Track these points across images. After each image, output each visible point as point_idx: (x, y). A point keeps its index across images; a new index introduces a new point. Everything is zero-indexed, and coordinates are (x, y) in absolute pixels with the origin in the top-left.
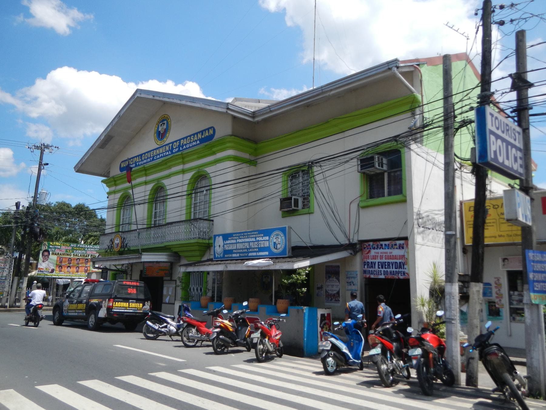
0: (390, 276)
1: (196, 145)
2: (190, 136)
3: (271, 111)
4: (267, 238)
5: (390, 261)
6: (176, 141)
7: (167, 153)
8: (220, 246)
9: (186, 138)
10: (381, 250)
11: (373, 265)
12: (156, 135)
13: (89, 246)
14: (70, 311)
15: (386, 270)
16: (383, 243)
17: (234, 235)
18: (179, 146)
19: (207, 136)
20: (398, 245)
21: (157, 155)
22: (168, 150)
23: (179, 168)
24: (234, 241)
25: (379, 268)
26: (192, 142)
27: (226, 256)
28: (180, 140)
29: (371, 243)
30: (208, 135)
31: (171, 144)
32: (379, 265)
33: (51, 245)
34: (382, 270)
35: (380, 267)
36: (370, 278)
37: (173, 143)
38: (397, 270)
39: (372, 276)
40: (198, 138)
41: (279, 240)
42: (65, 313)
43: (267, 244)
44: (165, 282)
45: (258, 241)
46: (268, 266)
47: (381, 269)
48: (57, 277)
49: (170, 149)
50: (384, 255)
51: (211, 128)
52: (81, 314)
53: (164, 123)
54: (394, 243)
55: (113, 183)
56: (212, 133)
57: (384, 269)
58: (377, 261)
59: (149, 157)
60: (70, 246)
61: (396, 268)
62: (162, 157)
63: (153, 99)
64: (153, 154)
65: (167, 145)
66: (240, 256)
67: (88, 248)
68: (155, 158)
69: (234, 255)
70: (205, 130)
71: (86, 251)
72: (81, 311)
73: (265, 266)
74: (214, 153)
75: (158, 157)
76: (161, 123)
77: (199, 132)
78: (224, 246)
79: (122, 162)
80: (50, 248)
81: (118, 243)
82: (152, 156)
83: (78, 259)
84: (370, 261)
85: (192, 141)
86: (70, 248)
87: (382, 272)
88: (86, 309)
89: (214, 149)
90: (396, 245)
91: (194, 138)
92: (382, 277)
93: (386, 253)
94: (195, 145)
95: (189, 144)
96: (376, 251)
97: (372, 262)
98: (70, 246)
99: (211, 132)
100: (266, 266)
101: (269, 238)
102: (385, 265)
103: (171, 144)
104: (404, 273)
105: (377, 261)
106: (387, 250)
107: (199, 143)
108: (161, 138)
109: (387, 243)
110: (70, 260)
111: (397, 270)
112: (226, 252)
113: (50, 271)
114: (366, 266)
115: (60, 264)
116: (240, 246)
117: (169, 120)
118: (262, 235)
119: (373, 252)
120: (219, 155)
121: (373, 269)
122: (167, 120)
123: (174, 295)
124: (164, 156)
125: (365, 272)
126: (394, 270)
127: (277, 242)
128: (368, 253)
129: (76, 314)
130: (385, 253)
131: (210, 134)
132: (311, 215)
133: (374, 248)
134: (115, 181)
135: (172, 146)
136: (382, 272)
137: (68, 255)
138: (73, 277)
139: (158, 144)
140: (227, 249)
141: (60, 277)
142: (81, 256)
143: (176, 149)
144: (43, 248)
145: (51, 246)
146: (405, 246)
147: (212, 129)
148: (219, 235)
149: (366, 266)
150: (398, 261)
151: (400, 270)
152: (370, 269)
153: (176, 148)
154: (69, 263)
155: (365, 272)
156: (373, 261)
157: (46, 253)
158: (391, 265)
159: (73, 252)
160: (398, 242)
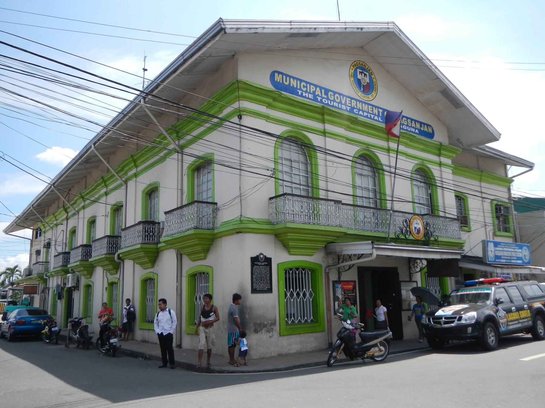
4: (520, 251)
8: (491, 251)
12: (352, 79)
14: (510, 323)
17: (501, 244)
22: (377, 114)
24: (501, 249)
27: (497, 260)
30: (427, 131)
40: (417, 128)
42: (504, 327)
43: (520, 255)
44: (402, 284)
45: (516, 252)
49: (381, 115)
52: (526, 324)
56: (431, 132)
62: (367, 117)
64: (351, 104)
66: (506, 262)
68: (355, 110)
69: (502, 261)
70: (424, 124)
72: (526, 320)
75: (361, 113)
76: (361, 71)
77: (418, 122)
78: (495, 252)
79: (279, 73)
88: (532, 316)
99: (430, 130)
107: (418, 133)
112: (497, 257)
116: (506, 254)
118: (518, 248)
124: (370, 118)
127: (526, 255)
129: (520, 325)
132: (469, 233)
139: (360, 95)
140: (497, 254)
148: (491, 242)
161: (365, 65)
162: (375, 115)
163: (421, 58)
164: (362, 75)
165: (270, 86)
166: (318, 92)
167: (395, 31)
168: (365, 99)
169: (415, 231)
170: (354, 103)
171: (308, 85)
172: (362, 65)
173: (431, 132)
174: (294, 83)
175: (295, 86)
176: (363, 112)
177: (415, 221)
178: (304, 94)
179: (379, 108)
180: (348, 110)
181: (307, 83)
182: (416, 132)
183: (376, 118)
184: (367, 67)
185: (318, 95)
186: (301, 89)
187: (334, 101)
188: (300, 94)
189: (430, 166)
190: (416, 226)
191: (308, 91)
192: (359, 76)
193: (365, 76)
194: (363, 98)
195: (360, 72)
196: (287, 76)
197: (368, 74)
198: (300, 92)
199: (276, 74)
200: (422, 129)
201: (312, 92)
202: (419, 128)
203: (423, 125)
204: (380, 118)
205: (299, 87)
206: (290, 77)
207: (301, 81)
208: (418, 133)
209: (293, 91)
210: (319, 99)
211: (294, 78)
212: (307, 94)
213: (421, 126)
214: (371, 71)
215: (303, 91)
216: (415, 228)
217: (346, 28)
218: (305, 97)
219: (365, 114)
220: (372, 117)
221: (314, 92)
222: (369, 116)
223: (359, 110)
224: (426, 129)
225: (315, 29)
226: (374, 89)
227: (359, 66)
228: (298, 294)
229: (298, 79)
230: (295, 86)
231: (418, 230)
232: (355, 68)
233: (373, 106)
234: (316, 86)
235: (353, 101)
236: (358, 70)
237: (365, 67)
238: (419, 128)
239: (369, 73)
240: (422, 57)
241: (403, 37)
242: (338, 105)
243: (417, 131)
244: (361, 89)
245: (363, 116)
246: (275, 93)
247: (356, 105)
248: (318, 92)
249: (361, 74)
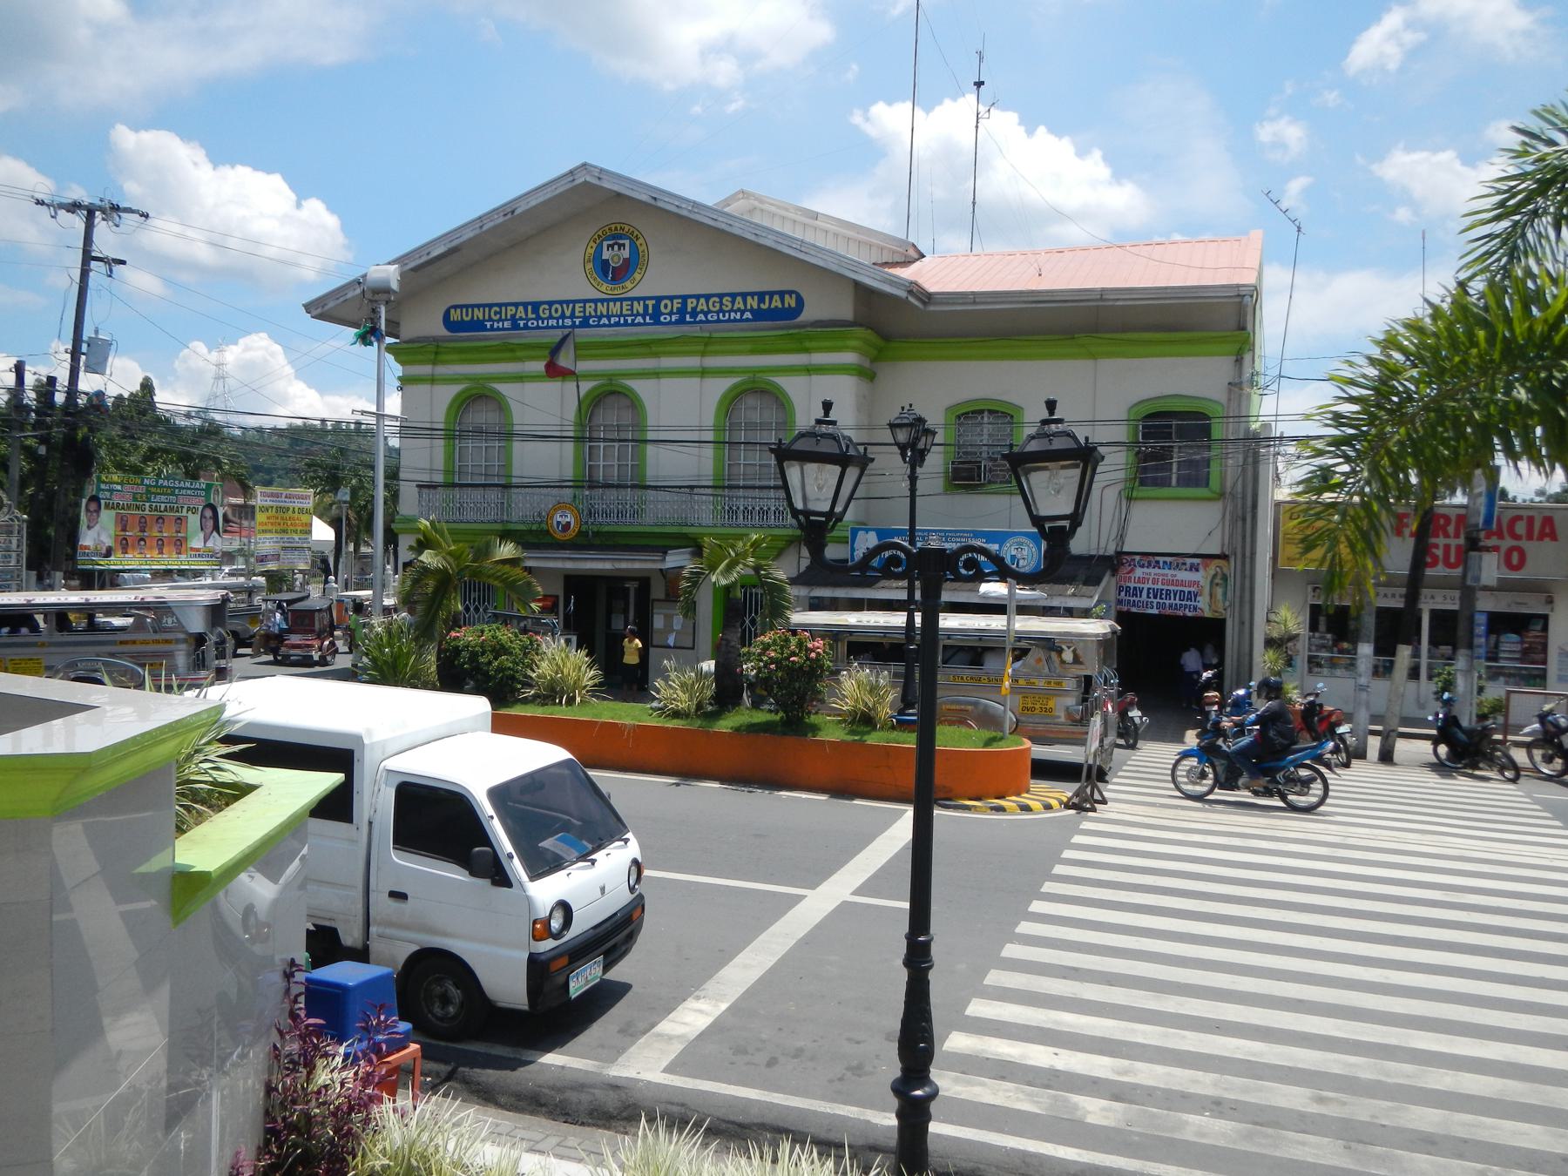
0: (1168, 612)
1: (741, 320)
2: (721, 296)
3: (975, 303)
5: (1171, 588)
6: (671, 298)
7: (639, 319)
9: (708, 297)
10: (1156, 570)
11: (1137, 592)
12: (590, 266)
13: (182, 485)
15: (1161, 601)
16: (1162, 559)
18: (682, 311)
19: (776, 307)
20: (1188, 566)
21: (600, 318)
22: (641, 311)
23: (693, 362)
25: (1148, 597)
26: (729, 312)
28: (685, 298)
29: (1137, 558)
30: (780, 306)
31: (654, 302)
32: (1148, 593)
33: (104, 482)
34: (1155, 601)
35: (1151, 595)
36: (1129, 613)
37: (659, 299)
38: (1183, 603)
39: (1134, 610)
40: (749, 307)
41: (1025, 553)
46: (1035, 600)
47: (1152, 600)
48: (121, 567)
49: (650, 311)
50: (1161, 578)
51: (790, 293)
53: (624, 245)
54: (1181, 560)
55: (432, 357)
56: (793, 304)
57: (1158, 600)
58: (1146, 586)
59: (568, 313)
60: (142, 484)
61: (1180, 600)
62: (617, 324)
63: (651, 205)
64: (584, 312)
65: (638, 299)
67: (180, 488)
68: (591, 322)
70: (772, 294)
71: (176, 495)
73: (1026, 600)
74: (807, 351)
76: (611, 242)
77: (752, 294)
79: (455, 307)
80: (103, 490)
81: (569, 523)
82: (577, 314)
83: (160, 517)
84: (1132, 585)
85: (724, 307)
86: (142, 489)
87: (1155, 605)
89: (807, 344)
90: (1184, 564)
91: (733, 302)
92: (1155, 611)
93: (1167, 575)
94: (735, 320)
95: (718, 313)
96: (1145, 570)
97: (1135, 588)
98: (142, 484)
99: (791, 302)
100: (1030, 600)
101: (1000, 547)
102: (1161, 594)
103: (654, 302)
104: (1195, 608)
105: (1146, 586)
106: (1166, 571)
107: (750, 317)
109: (1168, 559)
110: (143, 520)
111: (1183, 603)
113: (104, 551)
114: (1123, 594)
115: (123, 533)
117: (641, 240)
119: (1139, 572)
120: (819, 358)
121: (1137, 599)
122: (630, 238)
123: (691, 631)
125: (1120, 602)
126: (1178, 601)
128: (1128, 573)
130: (1163, 575)
131: (786, 305)
133: (1143, 566)
134: (436, 353)
135: (656, 307)
136: (1155, 605)
137: (138, 508)
138: (169, 567)
139: (603, 289)
141: (127, 567)
142: (166, 510)
143: (671, 314)
144: (90, 490)
145: (103, 486)
146: (1201, 567)
147: (794, 296)
149: (1123, 594)
150: (1186, 590)
151: (1188, 603)
152: (1132, 599)
153: (671, 314)
154: (141, 531)
155: (1120, 602)
156: (1137, 585)
157: (93, 506)
158: (1172, 595)
159: (149, 500)
160: (1189, 561)
162: (638, 314)
163: (652, 202)
164: (613, 249)
165: (443, 332)
166: (521, 312)
167: (589, 179)
170: (590, 308)
171: (503, 309)
173: (793, 304)
174: (478, 314)
175: (481, 318)
176: (609, 317)
178: (496, 325)
179: (644, 299)
180: (577, 323)
181: (500, 305)
182: (744, 317)
183: (639, 319)
184: (627, 228)
185: (521, 319)
186: (490, 319)
187: (551, 317)
188: (488, 327)
189: (776, 380)
190: (559, 519)
191: (503, 317)
192: (606, 255)
193: (619, 249)
195: (609, 246)
196: (467, 306)
197: (627, 242)
198: (488, 324)
199: (452, 311)
200: (764, 306)
201: (509, 317)
202: (755, 306)
203: (767, 298)
204: (648, 318)
205: (487, 317)
206: (473, 306)
207: (490, 306)
208: (750, 317)
209: (478, 325)
210: (522, 323)
211: (478, 306)
212: (501, 325)
213: (761, 300)
214: (636, 233)
215: (493, 321)
217: (481, 227)
218: (498, 329)
219: (613, 320)
220: (630, 321)
221: (513, 316)
222: (622, 322)
223: (602, 316)
224: (776, 303)
225: (428, 254)
228: (477, 609)
229: (484, 306)
230: (481, 318)
232: (598, 241)
233: (632, 299)
234: (516, 305)
235: (588, 305)
238: (755, 306)
239: (630, 238)
240: (655, 199)
242: (558, 323)
243: (748, 315)
244: (607, 277)
245: (610, 325)
247: (596, 310)
248: (521, 312)
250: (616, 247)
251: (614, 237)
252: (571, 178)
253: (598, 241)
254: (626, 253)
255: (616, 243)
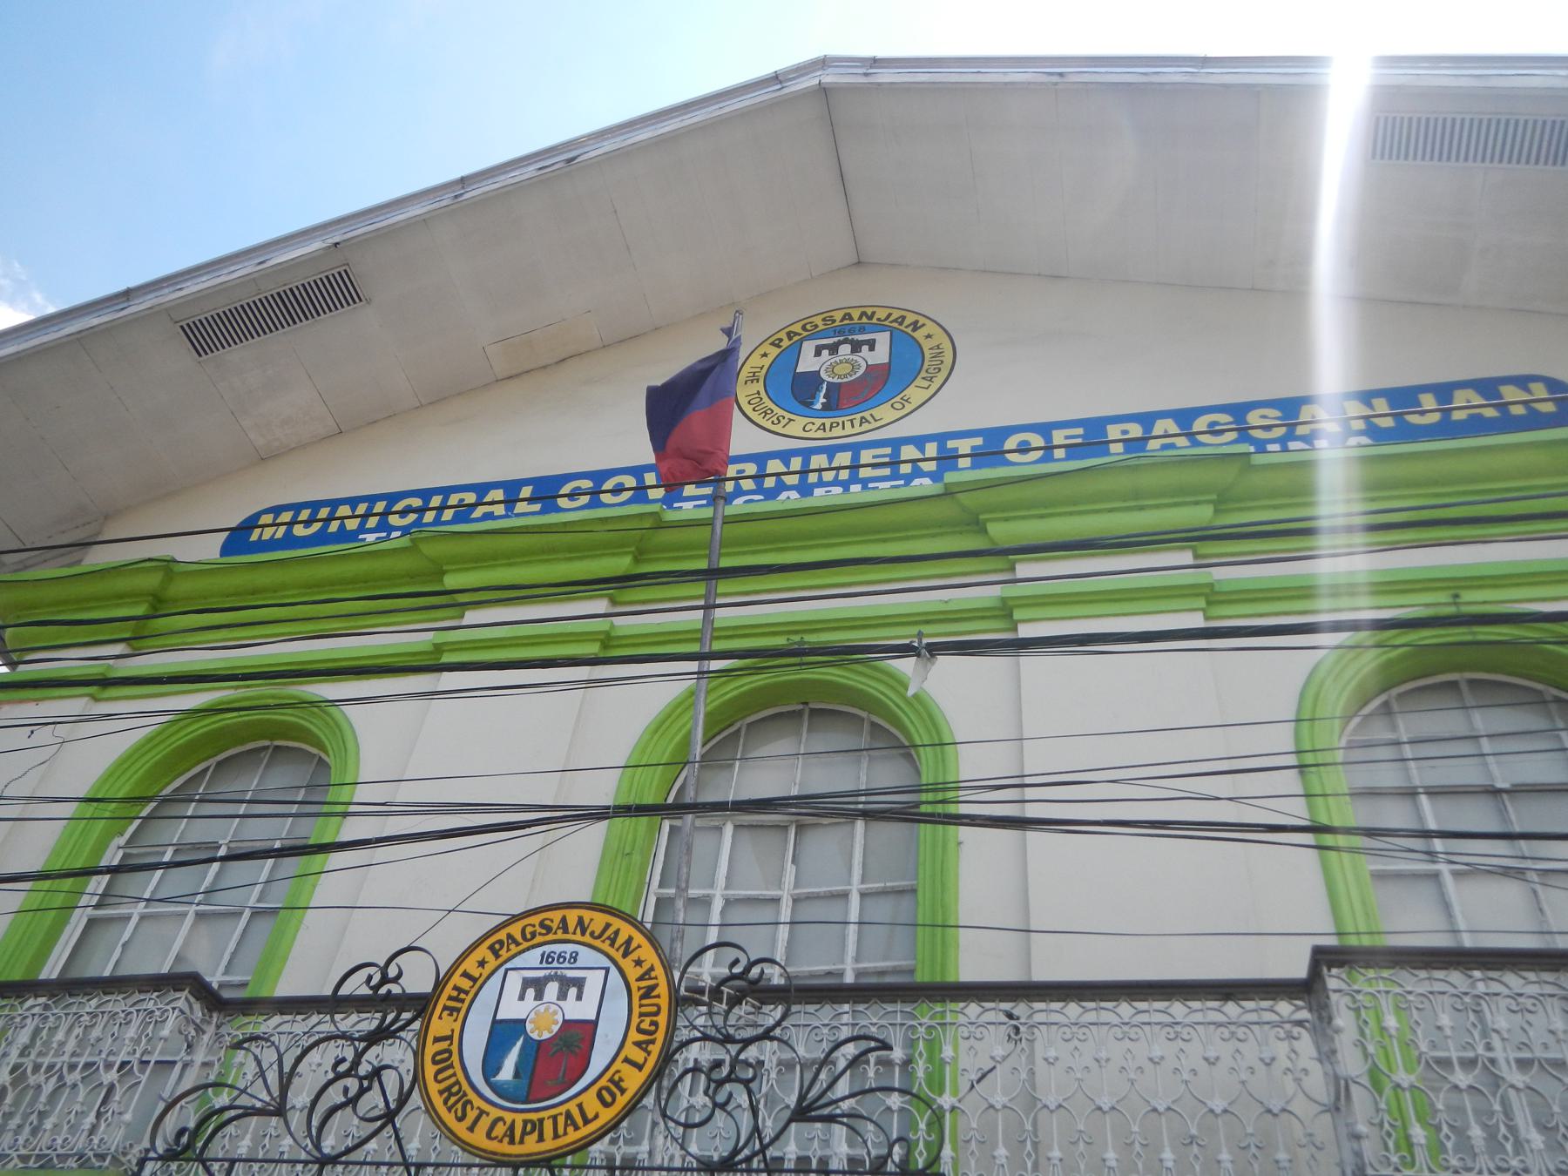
81: (579, 1036)
108: (826, 407)
117: (930, 328)
161: (869, 311)
168: (838, 432)
169: (491, 1065)
172: (848, 316)
177: (533, 957)
192: (808, 362)
194: (820, 434)
197: (883, 339)
216: (503, 1033)
226: (923, 374)
227: (821, 327)
231: (536, 1052)
232: (786, 343)
236: (809, 348)
237: (864, 320)
239: (892, 331)
240: (1061, 74)
241: (885, 76)
244: (809, 405)
246: (138, 569)
249: (825, 352)
250: (845, 349)
251: (838, 332)
252: (779, 87)
253: (786, 343)
254: (881, 355)
255: (845, 342)
